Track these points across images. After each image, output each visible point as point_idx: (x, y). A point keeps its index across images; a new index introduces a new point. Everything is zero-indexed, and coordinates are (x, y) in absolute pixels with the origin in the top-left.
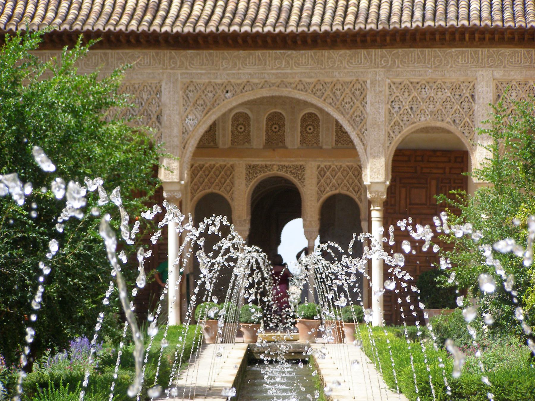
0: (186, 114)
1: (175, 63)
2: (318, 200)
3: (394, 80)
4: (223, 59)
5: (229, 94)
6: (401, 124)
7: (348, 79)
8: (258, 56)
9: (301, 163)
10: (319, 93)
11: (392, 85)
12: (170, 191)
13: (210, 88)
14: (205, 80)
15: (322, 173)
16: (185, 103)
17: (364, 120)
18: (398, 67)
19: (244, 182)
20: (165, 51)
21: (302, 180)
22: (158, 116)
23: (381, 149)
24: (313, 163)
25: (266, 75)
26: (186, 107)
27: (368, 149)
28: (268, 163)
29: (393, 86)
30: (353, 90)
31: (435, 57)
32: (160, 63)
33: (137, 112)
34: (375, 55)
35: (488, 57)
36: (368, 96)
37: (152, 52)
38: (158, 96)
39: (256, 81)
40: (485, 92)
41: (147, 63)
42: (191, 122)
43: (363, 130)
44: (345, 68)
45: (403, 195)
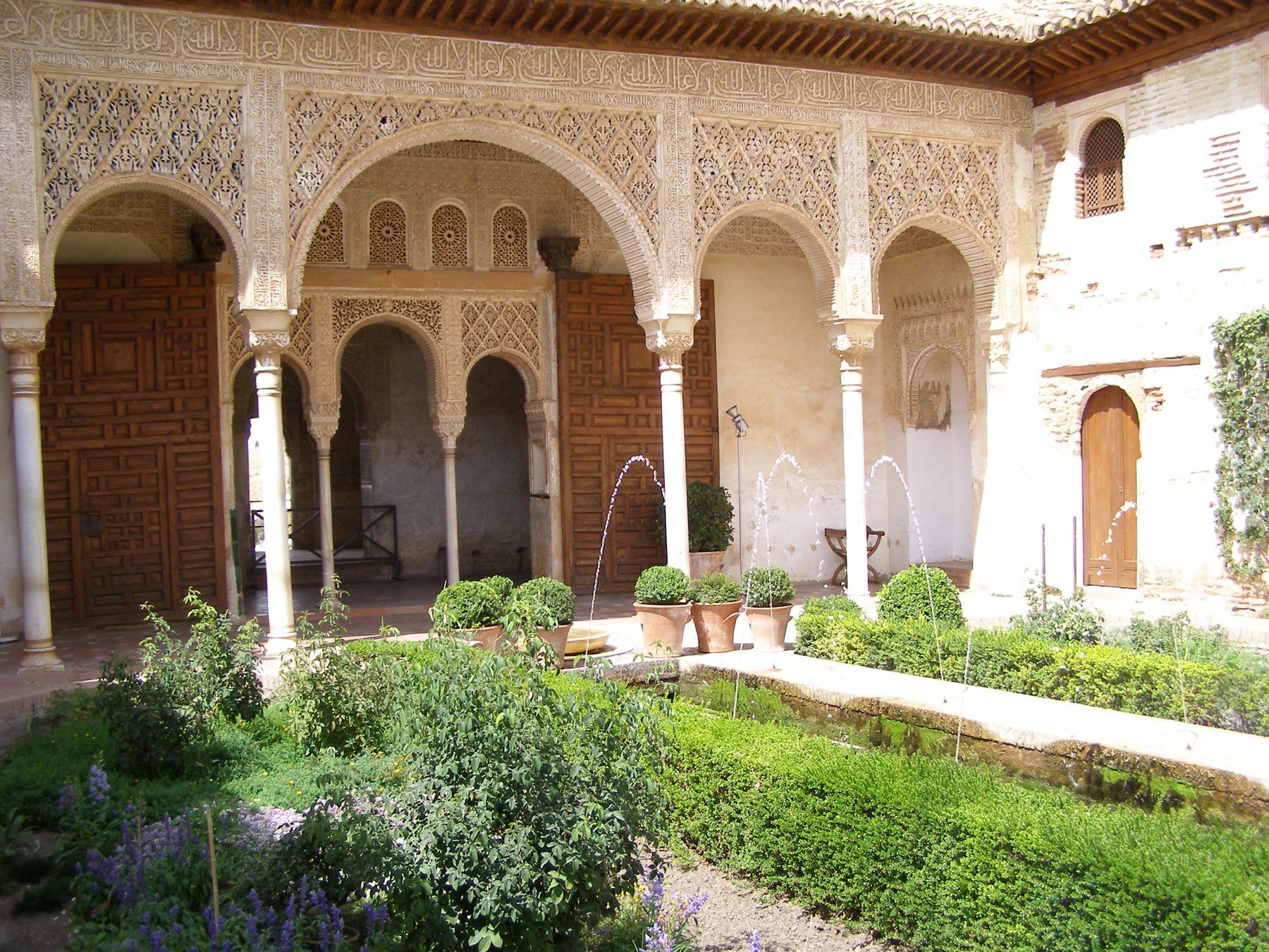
0: (297, 162)
1: (273, 49)
2: (465, 366)
3: (703, 119)
4: (378, 48)
5: (387, 125)
6: (718, 203)
7: (623, 110)
8: (451, 47)
9: (433, 298)
10: (566, 134)
11: (700, 128)
12: (266, 332)
13: (348, 110)
14: (338, 91)
15: (471, 316)
16: (294, 141)
17: (653, 193)
18: (712, 93)
19: (331, 332)
20: (251, 21)
21: (435, 327)
22: (234, 165)
23: (686, 250)
24: (455, 298)
25: (466, 89)
26: (297, 146)
27: (663, 250)
28: (376, 297)
29: (702, 131)
30: (631, 132)
31: (774, 82)
32: (239, 44)
33: (186, 154)
34: (671, 67)
35: (859, 90)
36: (658, 147)
37: (221, 20)
38: (234, 120)
39: (446, 100)
40: (853, 153)
41: (209, 42)
42: (309, 181)
43: (651, 212)
44: (618, 87)
45: (616, 357)
